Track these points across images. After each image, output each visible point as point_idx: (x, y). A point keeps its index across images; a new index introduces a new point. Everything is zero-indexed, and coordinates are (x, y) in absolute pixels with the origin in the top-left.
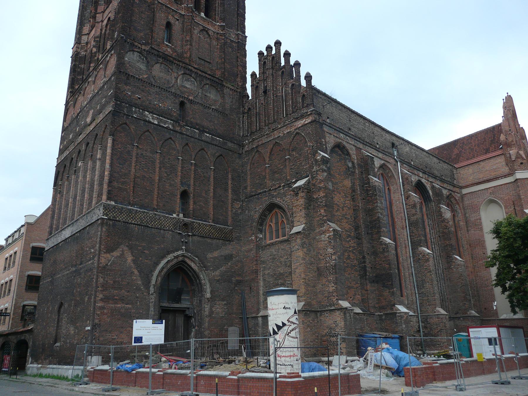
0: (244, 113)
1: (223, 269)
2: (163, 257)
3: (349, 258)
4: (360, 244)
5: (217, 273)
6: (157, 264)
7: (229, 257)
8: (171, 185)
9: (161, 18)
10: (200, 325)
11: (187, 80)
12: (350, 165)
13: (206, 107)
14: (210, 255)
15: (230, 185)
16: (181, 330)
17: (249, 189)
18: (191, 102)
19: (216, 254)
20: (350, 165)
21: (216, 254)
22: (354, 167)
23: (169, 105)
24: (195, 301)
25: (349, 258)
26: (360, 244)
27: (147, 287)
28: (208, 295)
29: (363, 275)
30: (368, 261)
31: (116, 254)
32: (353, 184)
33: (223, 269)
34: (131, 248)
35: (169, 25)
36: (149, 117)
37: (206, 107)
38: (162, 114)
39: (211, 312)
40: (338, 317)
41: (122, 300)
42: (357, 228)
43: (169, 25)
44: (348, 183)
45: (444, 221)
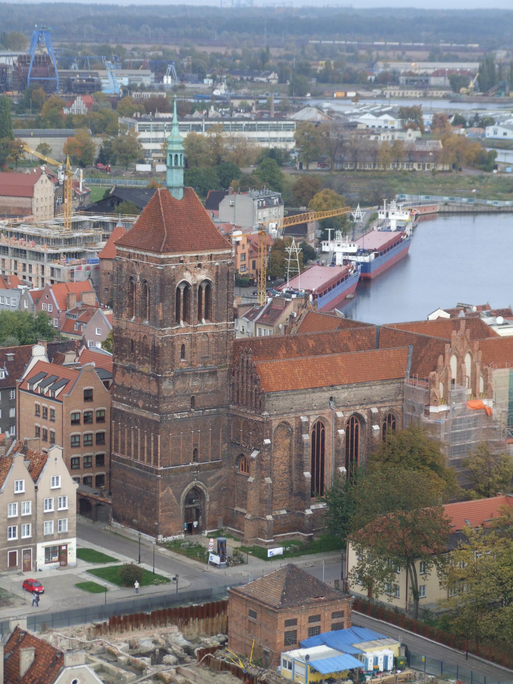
0: (230, 385)
1: (216, 484)
2: (186, 486)
3: (283, 484)
4: (291, 476)
5: (213, 487)
6: (183, 491)
7: (220, 477)
8: (188, 448)
9: (178, 344)
10: (204, 514)
11: (195, 381)
12: (290, 430)
13: (205, 393)
14: (209, 479)
15: (221, 435)
16: (195, 515)
17: (232, 437)
18: (198, 394)
19: (212, 478)
20: (290, 430)
21: (212, 478)
22: (292, 431)
23: (186, 403)
24: (202, 503)
25: (283, 484)
26: (291, 476)
27: (179, 502)
28: (208, 500)
29: (291, 493)
30: (294, 485)
31: (165, 491)
32: (291, 441)
33: (216, 484)
34: (171, 486)
35: (183, 346)
36: (177, 416)
37: (205, 393)
38: (182, 410)
39: (210, 508)
40: (265, 523)
41: (169, 511)
42: (290, 467)
43: (183, 346)
44: (287, 441)
45: (372, 437)
